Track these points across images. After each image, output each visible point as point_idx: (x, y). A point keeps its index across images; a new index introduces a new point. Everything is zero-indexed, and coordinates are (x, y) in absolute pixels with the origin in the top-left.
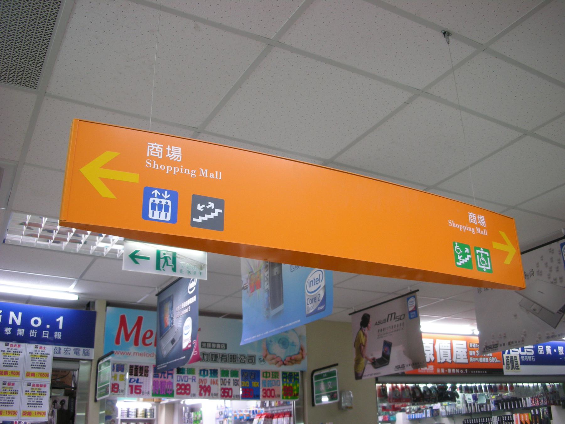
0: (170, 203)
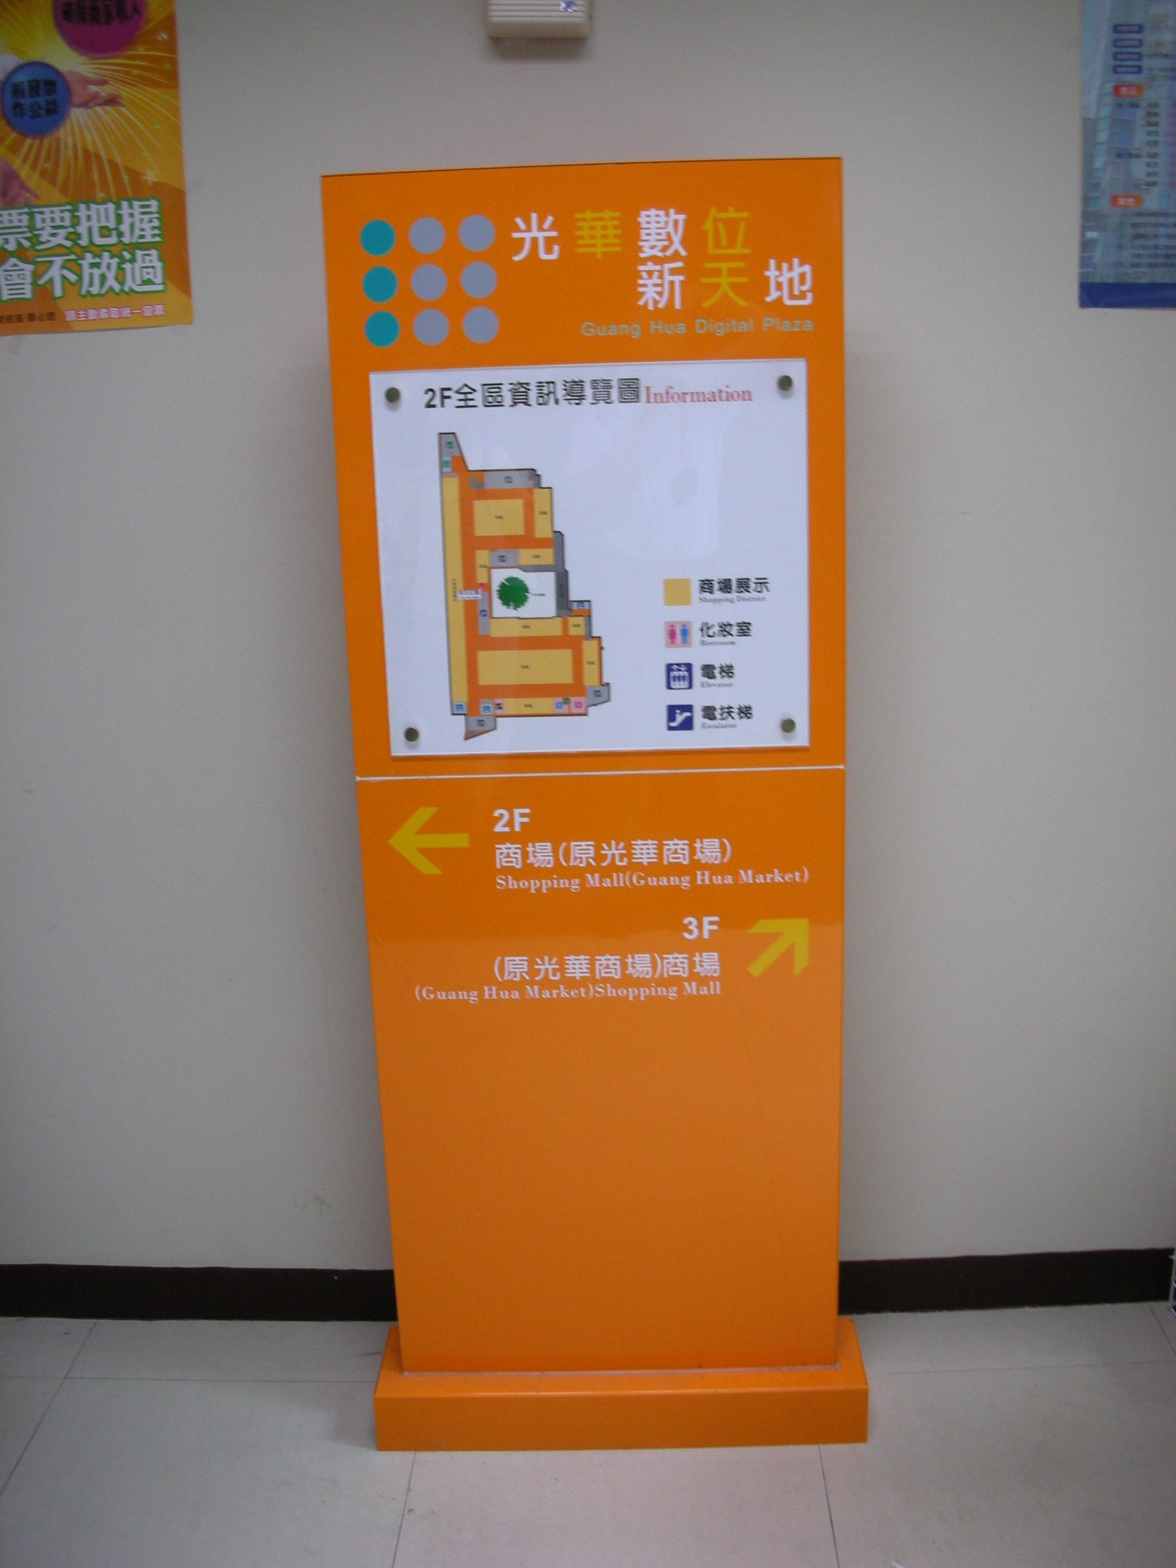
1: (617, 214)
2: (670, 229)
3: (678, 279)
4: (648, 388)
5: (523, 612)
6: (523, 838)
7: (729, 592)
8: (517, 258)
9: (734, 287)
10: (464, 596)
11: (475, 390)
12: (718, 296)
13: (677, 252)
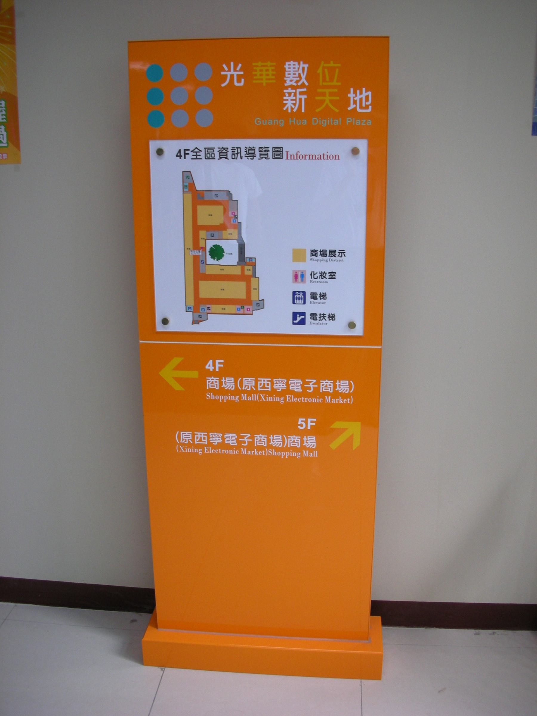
0: (303, 297)
1: (274, 64)
2: (301, 71)
3: (304, 97)
4: (287, 152)
5: (221, 262)
6: (220, 374)
7: (326, 257)
8: (223, 85)
9: (331, 101)
10: (193, 253)
11: (201, 151)
12: (325, 104)
13: (303, 83)
